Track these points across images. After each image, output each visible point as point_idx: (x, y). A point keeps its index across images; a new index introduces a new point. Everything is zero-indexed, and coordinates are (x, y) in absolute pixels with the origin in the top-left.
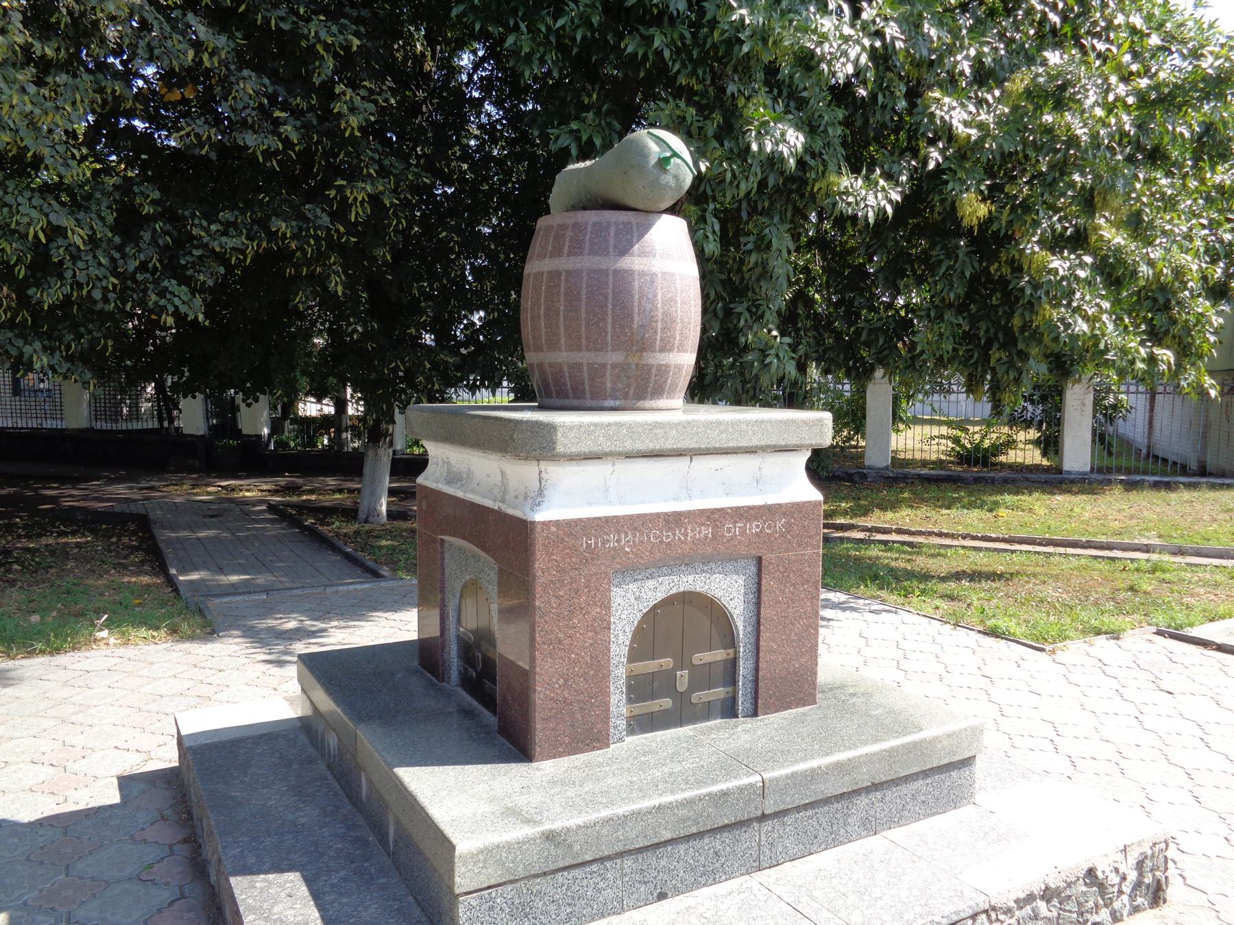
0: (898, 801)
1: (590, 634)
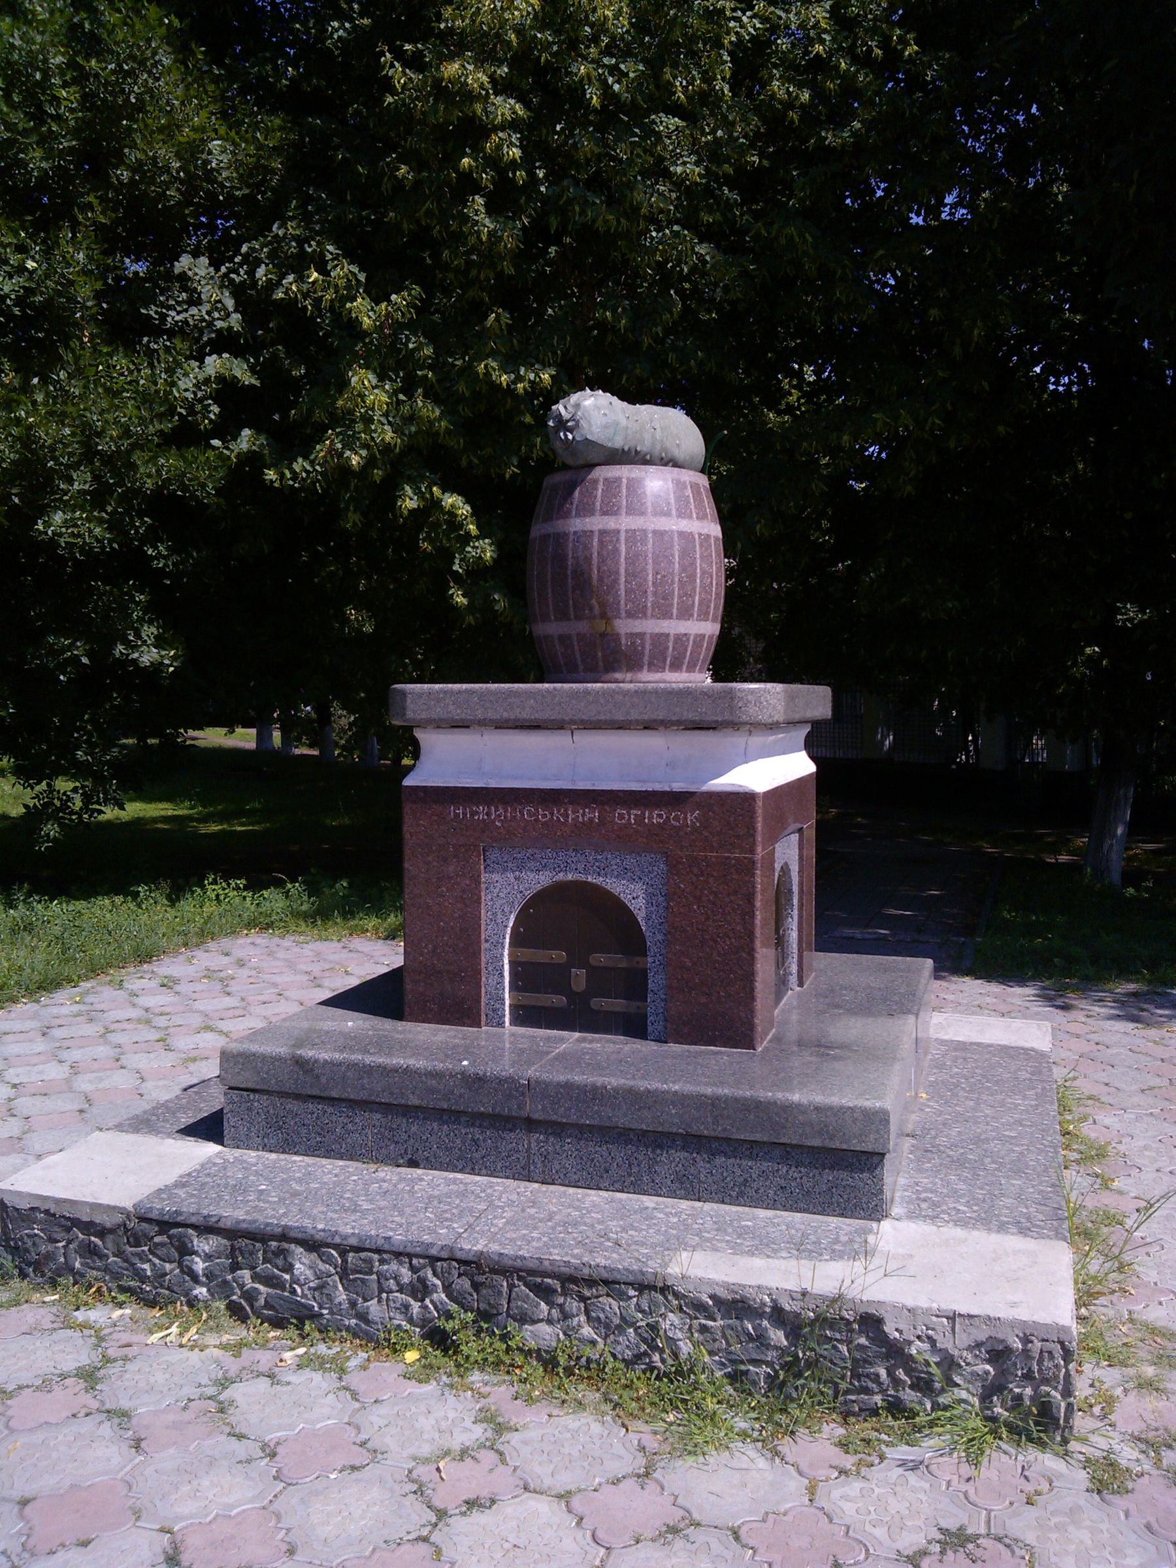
0: (739, 1172)
1: (459, 905)
